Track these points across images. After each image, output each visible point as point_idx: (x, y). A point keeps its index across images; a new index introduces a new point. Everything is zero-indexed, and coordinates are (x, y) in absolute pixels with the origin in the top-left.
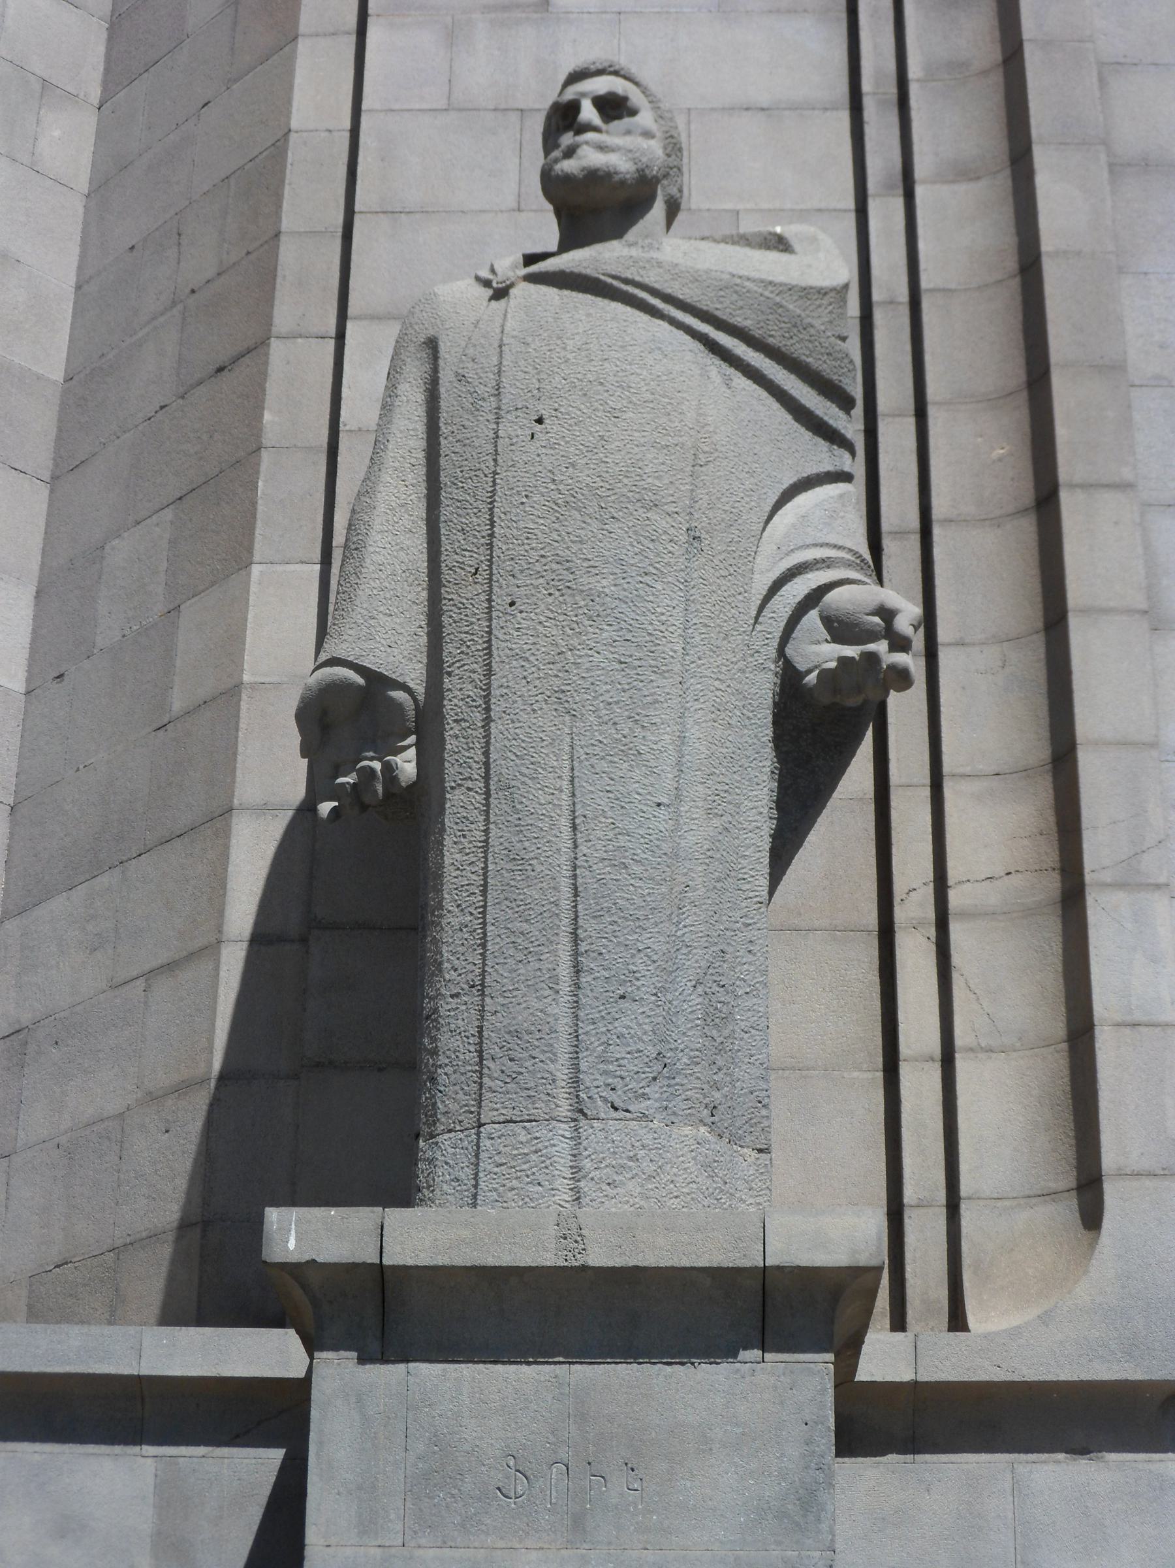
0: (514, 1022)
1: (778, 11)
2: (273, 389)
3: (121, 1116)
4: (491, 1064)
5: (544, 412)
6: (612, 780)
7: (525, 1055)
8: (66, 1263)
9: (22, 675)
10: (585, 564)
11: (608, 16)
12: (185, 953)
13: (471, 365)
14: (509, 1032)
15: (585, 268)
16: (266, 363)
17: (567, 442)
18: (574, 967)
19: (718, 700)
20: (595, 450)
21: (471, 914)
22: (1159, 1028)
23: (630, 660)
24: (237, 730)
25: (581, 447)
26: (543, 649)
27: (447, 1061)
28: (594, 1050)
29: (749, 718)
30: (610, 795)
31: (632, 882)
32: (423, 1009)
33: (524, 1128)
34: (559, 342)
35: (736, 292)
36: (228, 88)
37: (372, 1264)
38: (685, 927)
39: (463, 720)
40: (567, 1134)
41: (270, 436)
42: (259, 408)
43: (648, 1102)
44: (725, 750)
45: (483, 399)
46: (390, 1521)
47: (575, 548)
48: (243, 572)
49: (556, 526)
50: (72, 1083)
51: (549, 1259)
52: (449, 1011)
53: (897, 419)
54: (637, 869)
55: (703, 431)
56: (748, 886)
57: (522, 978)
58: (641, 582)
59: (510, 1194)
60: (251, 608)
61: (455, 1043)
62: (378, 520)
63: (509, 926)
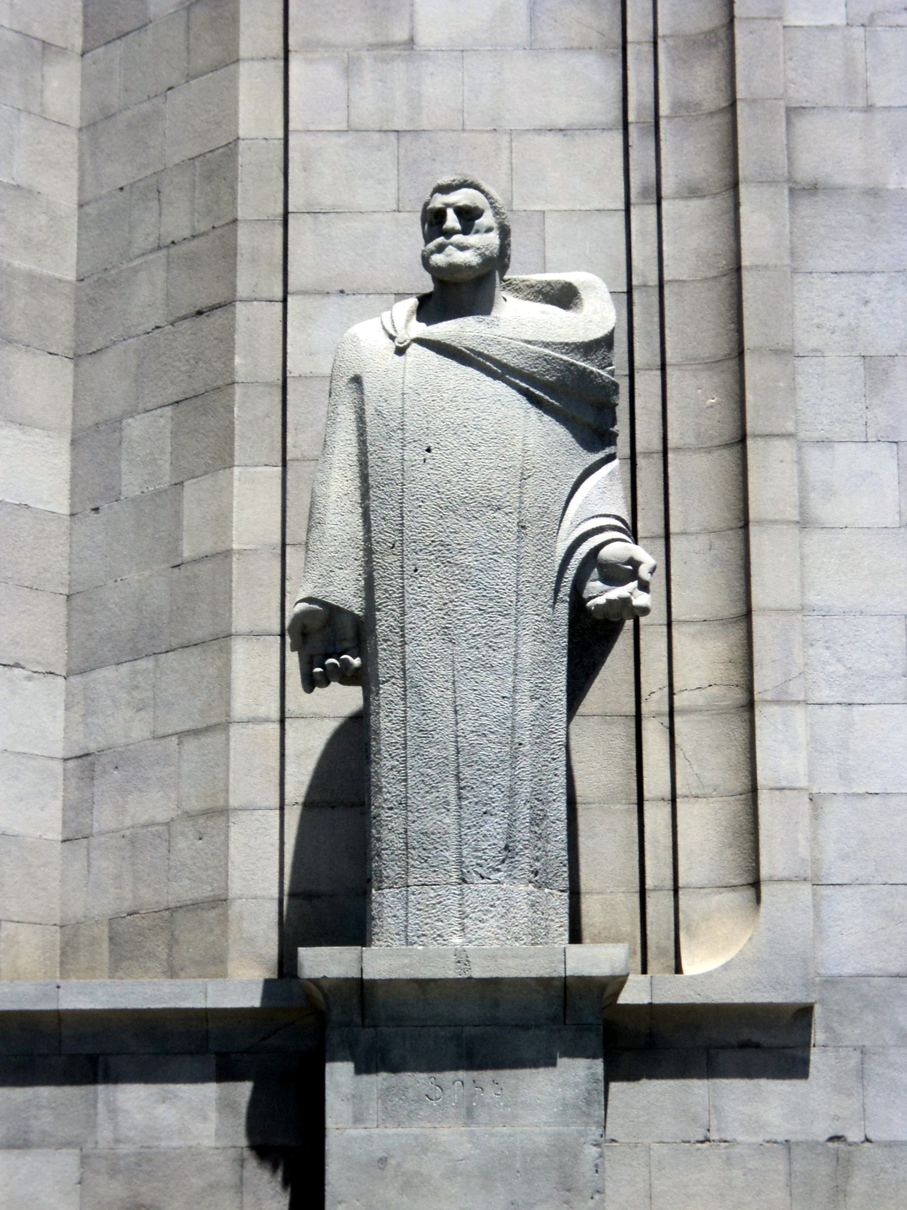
0: (425, 827)
1: (572, 48)
2: (240, 339)
3: (167, 824)
4: (412, 851)
5: (431, 445)
6: (477, 682)
7: (431, 847)
8: (136, 913)
9: (67, 502)
10: (459, 547)
11: (455, 54)
12: (205, 725)
13: (384, 404)
14: (422, 833)
15: (453, 341)
16: (234, 319)
17: (446, 466)
18: (458, 795)
19: (536, 627)
20: (463, 472)
21: (398, 761)
22: (796, 791)
23: (485, 608)
24: (231, 581)
25: (454, 470)
26: (435, 601)
27: (387, 847)
28: (470, 845)
29: (555, 632)
30: (476, 692)
31: (489, 745)
32: (371, 812)
33: (433, 889)
34: (438, 395)
35: (545, 360)
36: (187, 81)
37: (357, 979)
38: (519, 769)
39: (388, 640)
40: (456, 892)
41: (240, 375)
42: (230, 352)
43: (501, 873)
44: (539, 658)
45: (393, 431)
46: (370, 1114)
47: (452, 536)
48: (227, 471)
49: (440, 521)
50: (130, 796)
51: (452, 974)
52: (387, 817)
53: (647, 372)
54: (492, 736)
55: (526, 455)
56: (554, 736)
57: (429, 801)
58: (491, 559)
59: (426, 927)
60: (235, 498)
61: (392, 837)
62: (332, 506)
63: (420, 770)
